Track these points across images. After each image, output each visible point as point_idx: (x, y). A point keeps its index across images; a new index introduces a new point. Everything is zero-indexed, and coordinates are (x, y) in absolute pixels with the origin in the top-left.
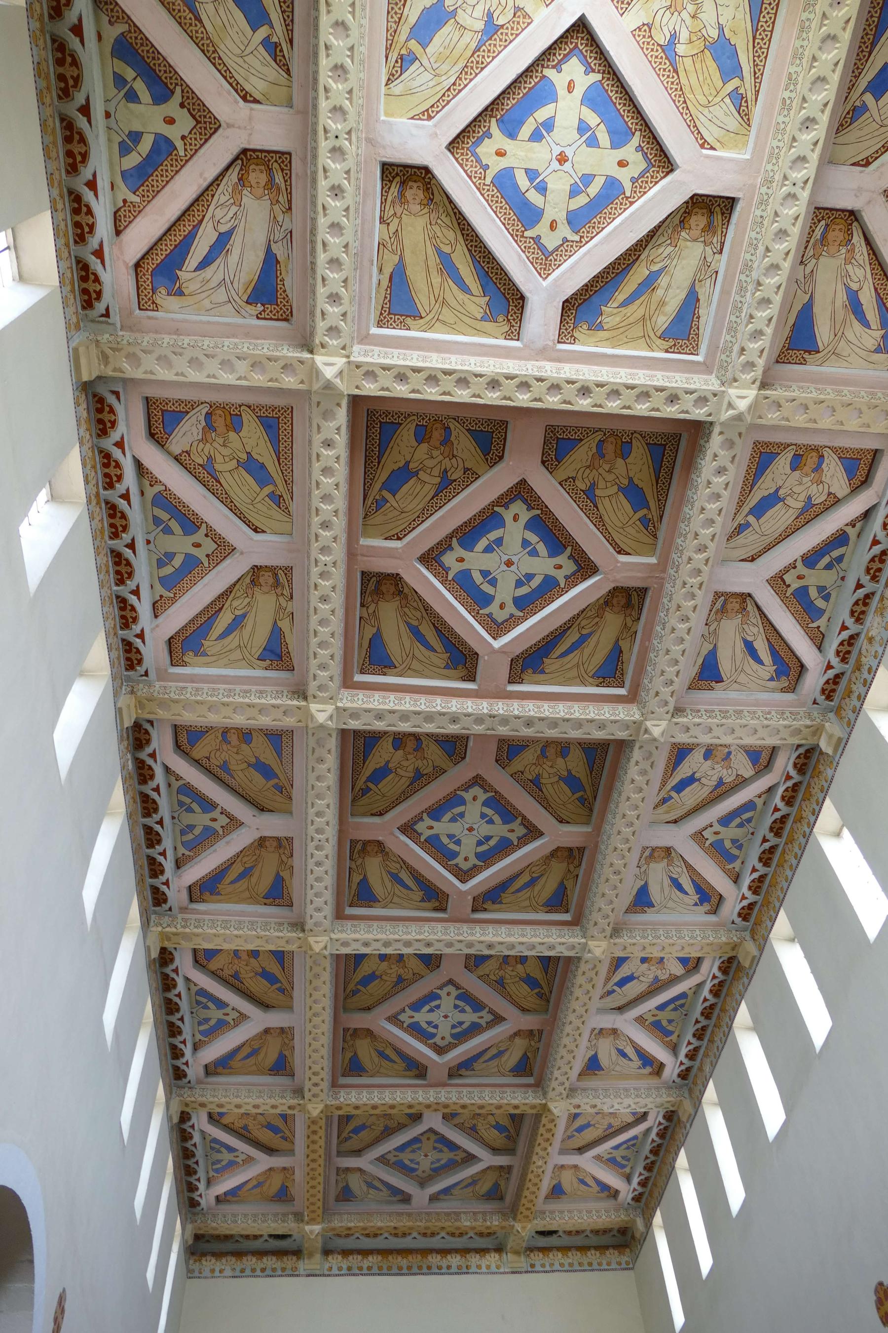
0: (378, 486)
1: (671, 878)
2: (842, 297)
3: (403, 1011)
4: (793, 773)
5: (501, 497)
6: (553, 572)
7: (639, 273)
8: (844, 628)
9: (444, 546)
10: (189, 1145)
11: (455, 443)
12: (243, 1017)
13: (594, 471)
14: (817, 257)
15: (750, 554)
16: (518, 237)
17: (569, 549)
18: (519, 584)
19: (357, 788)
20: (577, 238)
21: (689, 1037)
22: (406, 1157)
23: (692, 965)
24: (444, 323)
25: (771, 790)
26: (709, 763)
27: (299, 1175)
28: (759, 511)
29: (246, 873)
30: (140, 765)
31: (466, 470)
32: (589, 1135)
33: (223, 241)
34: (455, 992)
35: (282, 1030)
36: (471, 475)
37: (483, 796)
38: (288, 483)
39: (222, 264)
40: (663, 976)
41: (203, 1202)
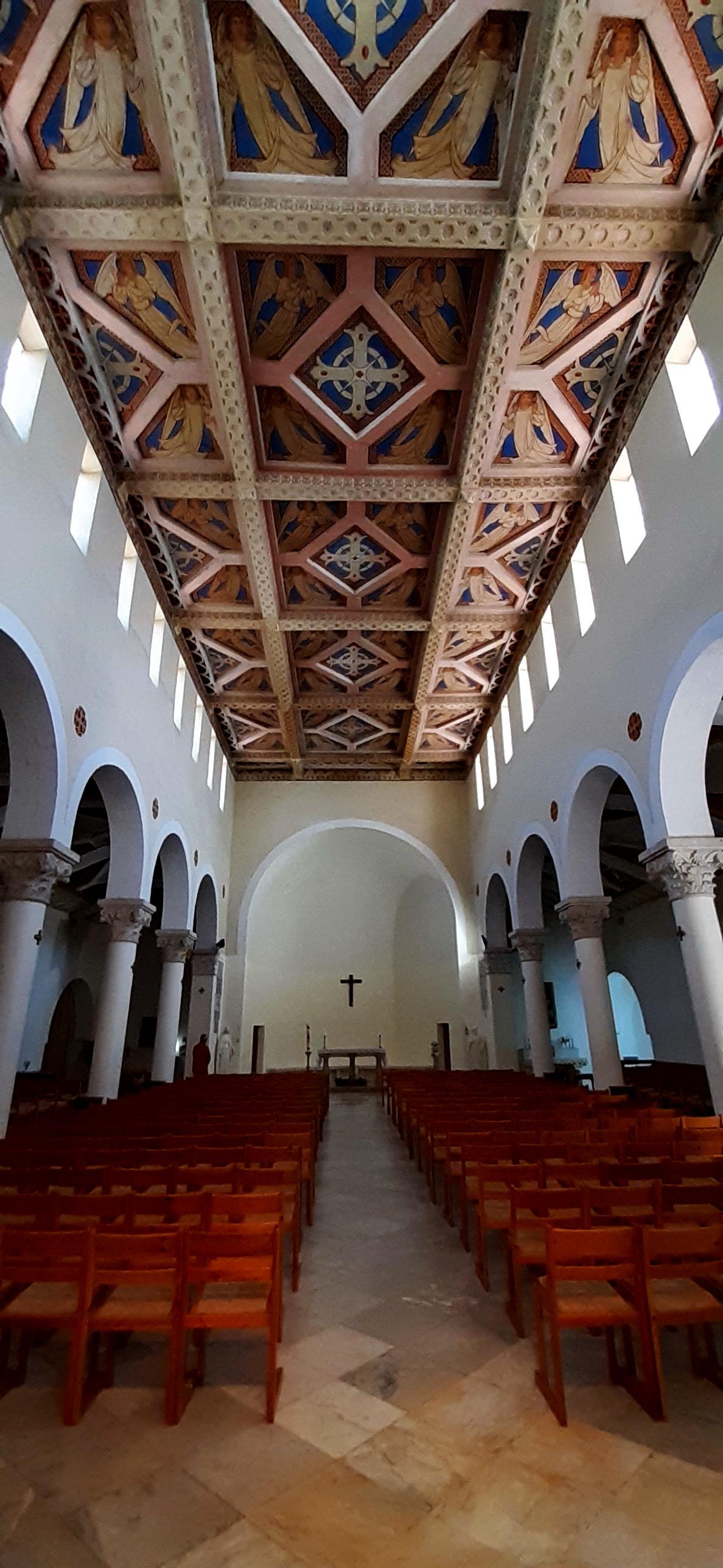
0: (256, 315)
1: (485, 585)
2: (626, 111)
3: (328, 659)
4: (564, 519)
5: (348, 321)
6: (391, 380)
7: (444, 99)
8: (608, 414)
9: (311, 363)
10: (223, 723)
11: (307, 275)
12: (237, 663)
14: (604, 68)
15: (540, 358)
16: (334, 66)
18: (368, 390)
19: (280, 535)
20: (387, 64)
21: (497, 672)
22: (341, 729)
23: (499, 635)
24: (284, 163)
25: (551, 530)
26: (508, 513)
27: (284, 736)
28: (546, 322)
29: (222, 586)
30: (140, 523)
31: (319, 299)
32: (442, 719)
33: (89, 92)
34: (357, 649)
35: (262, 669)
36: (322, 305)
37: (360, 538)
39: (94, 119)
40: (481, 640)
41: (237, 748)
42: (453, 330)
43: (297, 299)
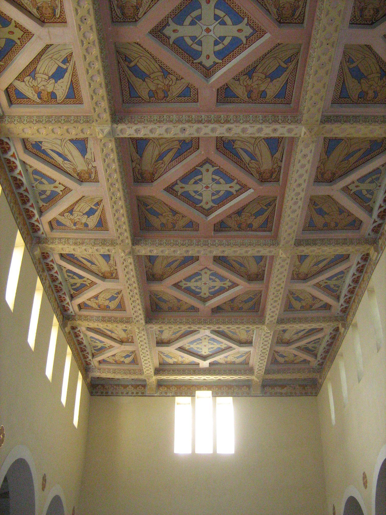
6: (178, 27)
13: (166, 84)
17: (171, 43)
31: (239, 80)
38: (341, 68)
42: (132, 64)
43: (254, 80)
